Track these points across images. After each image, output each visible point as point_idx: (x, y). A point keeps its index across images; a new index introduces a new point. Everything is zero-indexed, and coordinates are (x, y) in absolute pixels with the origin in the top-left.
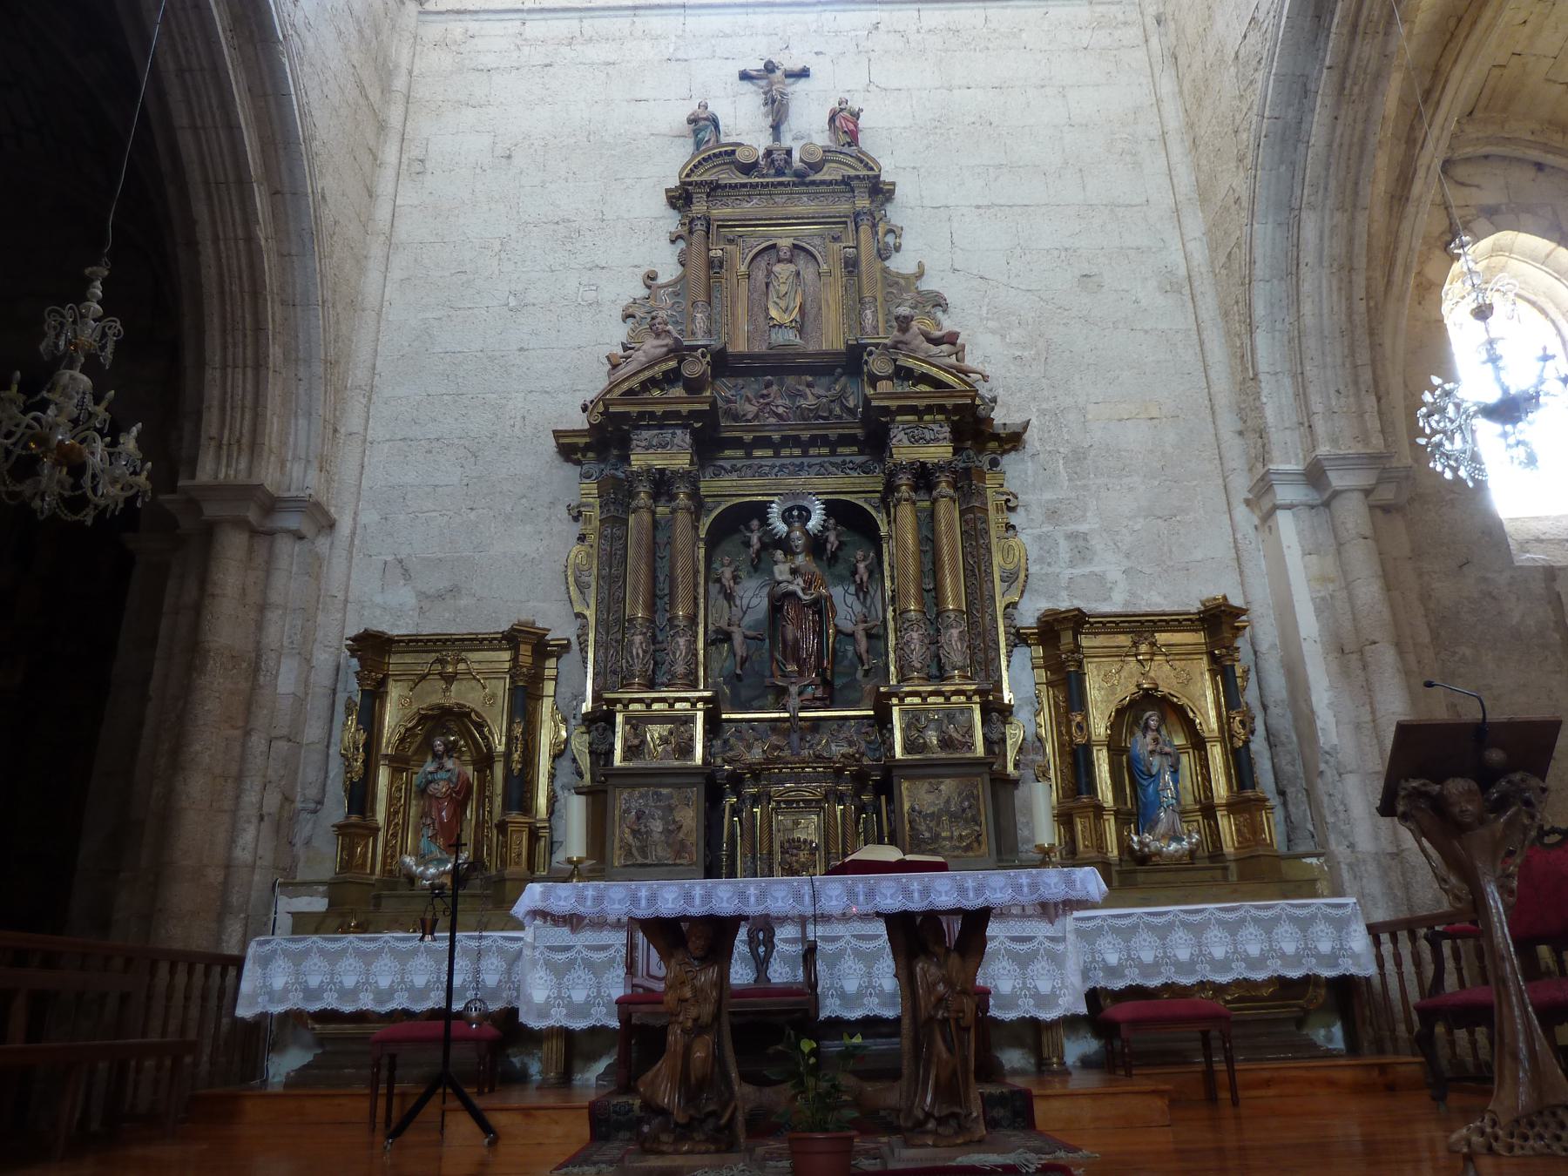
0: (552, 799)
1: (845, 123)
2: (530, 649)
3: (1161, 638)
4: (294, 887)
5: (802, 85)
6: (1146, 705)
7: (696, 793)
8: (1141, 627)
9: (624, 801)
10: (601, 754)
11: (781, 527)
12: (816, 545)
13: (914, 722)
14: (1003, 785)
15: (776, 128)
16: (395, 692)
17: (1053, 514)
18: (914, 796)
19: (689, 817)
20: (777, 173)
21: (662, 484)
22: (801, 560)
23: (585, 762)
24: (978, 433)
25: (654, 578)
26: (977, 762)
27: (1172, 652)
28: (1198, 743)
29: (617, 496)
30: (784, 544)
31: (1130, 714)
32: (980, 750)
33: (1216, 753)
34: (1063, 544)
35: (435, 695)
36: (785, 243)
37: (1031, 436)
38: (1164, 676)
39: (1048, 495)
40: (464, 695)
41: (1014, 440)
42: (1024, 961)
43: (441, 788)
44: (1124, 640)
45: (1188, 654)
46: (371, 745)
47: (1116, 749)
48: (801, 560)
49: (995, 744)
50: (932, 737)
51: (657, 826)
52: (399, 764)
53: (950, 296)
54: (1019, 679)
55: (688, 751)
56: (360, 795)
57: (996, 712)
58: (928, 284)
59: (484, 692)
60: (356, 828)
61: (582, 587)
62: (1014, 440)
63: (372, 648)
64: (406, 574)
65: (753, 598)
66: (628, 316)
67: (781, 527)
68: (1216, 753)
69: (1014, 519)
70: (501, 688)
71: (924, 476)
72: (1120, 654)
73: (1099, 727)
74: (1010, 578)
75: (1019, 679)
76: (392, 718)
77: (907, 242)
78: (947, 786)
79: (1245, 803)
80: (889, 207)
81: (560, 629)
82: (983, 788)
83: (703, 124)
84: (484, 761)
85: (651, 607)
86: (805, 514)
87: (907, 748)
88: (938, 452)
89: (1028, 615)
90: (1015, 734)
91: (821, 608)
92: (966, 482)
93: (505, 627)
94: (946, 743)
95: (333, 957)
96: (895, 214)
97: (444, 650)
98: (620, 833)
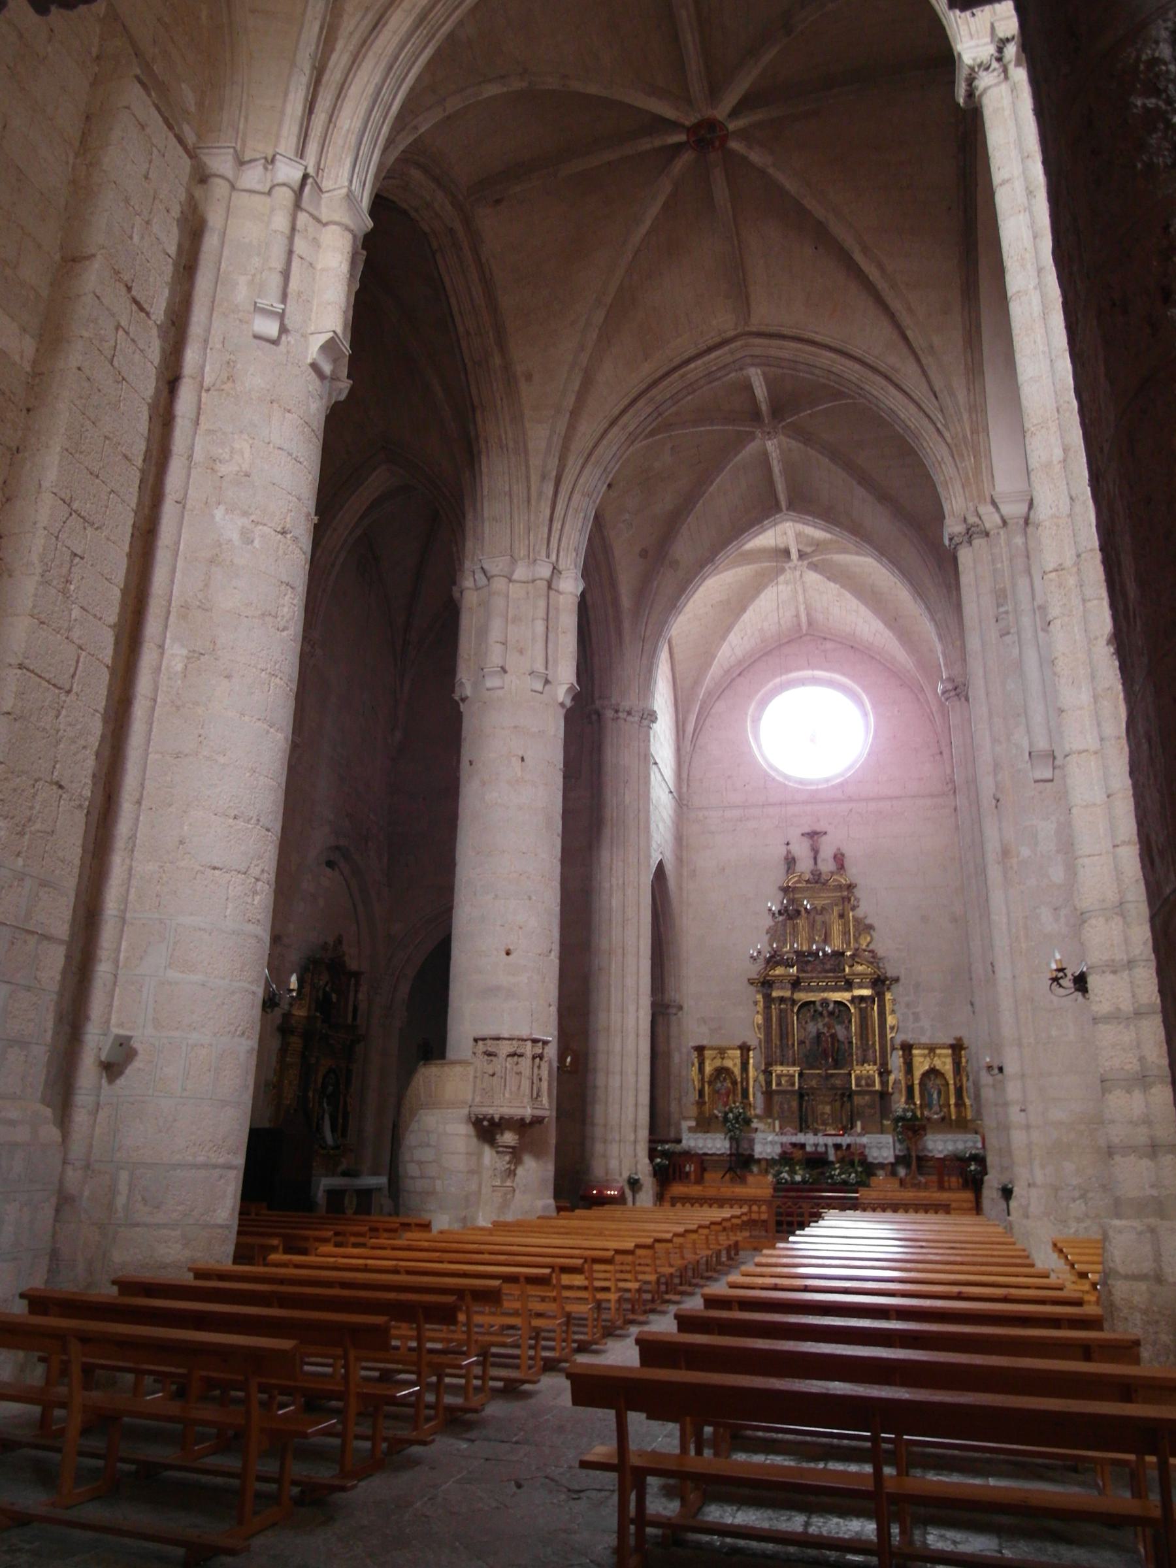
0: (754, 1094)
1: (839, 859)
2: (745, 1049)
3: (938, 1051)
4: (685, 1118)
5: (824, 838)
6: (933, 1072)
7: (796, 1097)
8: (932, 1049)
9: (777, 1099)
10: (769, 1083)
11: (820, 1009)
12: (831, 1014)
13: (858, 1078)
14: (884, 1096)
15: (815, 859)
16: (707, 1062)
17: (908, 1005)
18: (858, 1100)
19: (795, 1104)
20: (817, 879)
21: (782, 1000)
22: (826, 1020)
23: (763, 1084)
24: (880, 983)
25: (781, 1030)
26: (876, 1091)
27: (940, 1056)
28: (948, 1084)
29: (768, 999)
30: (821, 1014)
31: (926, 1075)
32: (878, 1087)
33: (952, 1088)
34: (911, 1018)
35: (718, 1063)
36: (819, 908)
37: (902, 980)
38: (938, 1063)
39: (907, 999)
40: (728, 1063)
41: (897, 980)
42: (880, 1148)
43: (723, 1091)
44: (926, 1052)
45: (946, 1056)
46: (703, 1079)
47: (921, 1084)
48: (826, 1020)
49: (884, 1083)
50: (863, 1082)
51: (786, 1106)
52: (710, 1083)
53: (876, 925)
54: (896, 1060)
55: (793, 1084)
56: (701, 1093)
57: (884, 1073)
58: (868, 921)
59: (733, 1061)
60: (701, 1103)
61: (759, 1028)
62: (897, 980)
63: (700, 1050)
64: (705, 1023)
65: (812, 1028)
66: (767, 933)
67: (820, 1009)
68: (952, 1088)
69: (896, 1008)
70: (738, 1061)
71: (862, 999)
72: (925, 1056)
73: (917, 1074)
74: (892, 1028)
75: (896, 1060)
76: (708, 1069)
77: (862, 904)
78: (867, 1098)
79: (960, 1103)
80: (855, 890)
81: (753, 1043)
82: (877, 1099)
83: (790, 862)
84: (734, 1083)
85: (781, 1040)
86: (828, 1005)
87: (857, 1085)
88: (866, 992)
89: (898, 1042)
90: (892, 1078)
91: (834, 1036)
92: (880, 995)
93: (739, 1044)
94: (868, 1085)
95: (714, 1139)
96: (858, 892)
97: (722, 1052)
98: (776, 1109)
